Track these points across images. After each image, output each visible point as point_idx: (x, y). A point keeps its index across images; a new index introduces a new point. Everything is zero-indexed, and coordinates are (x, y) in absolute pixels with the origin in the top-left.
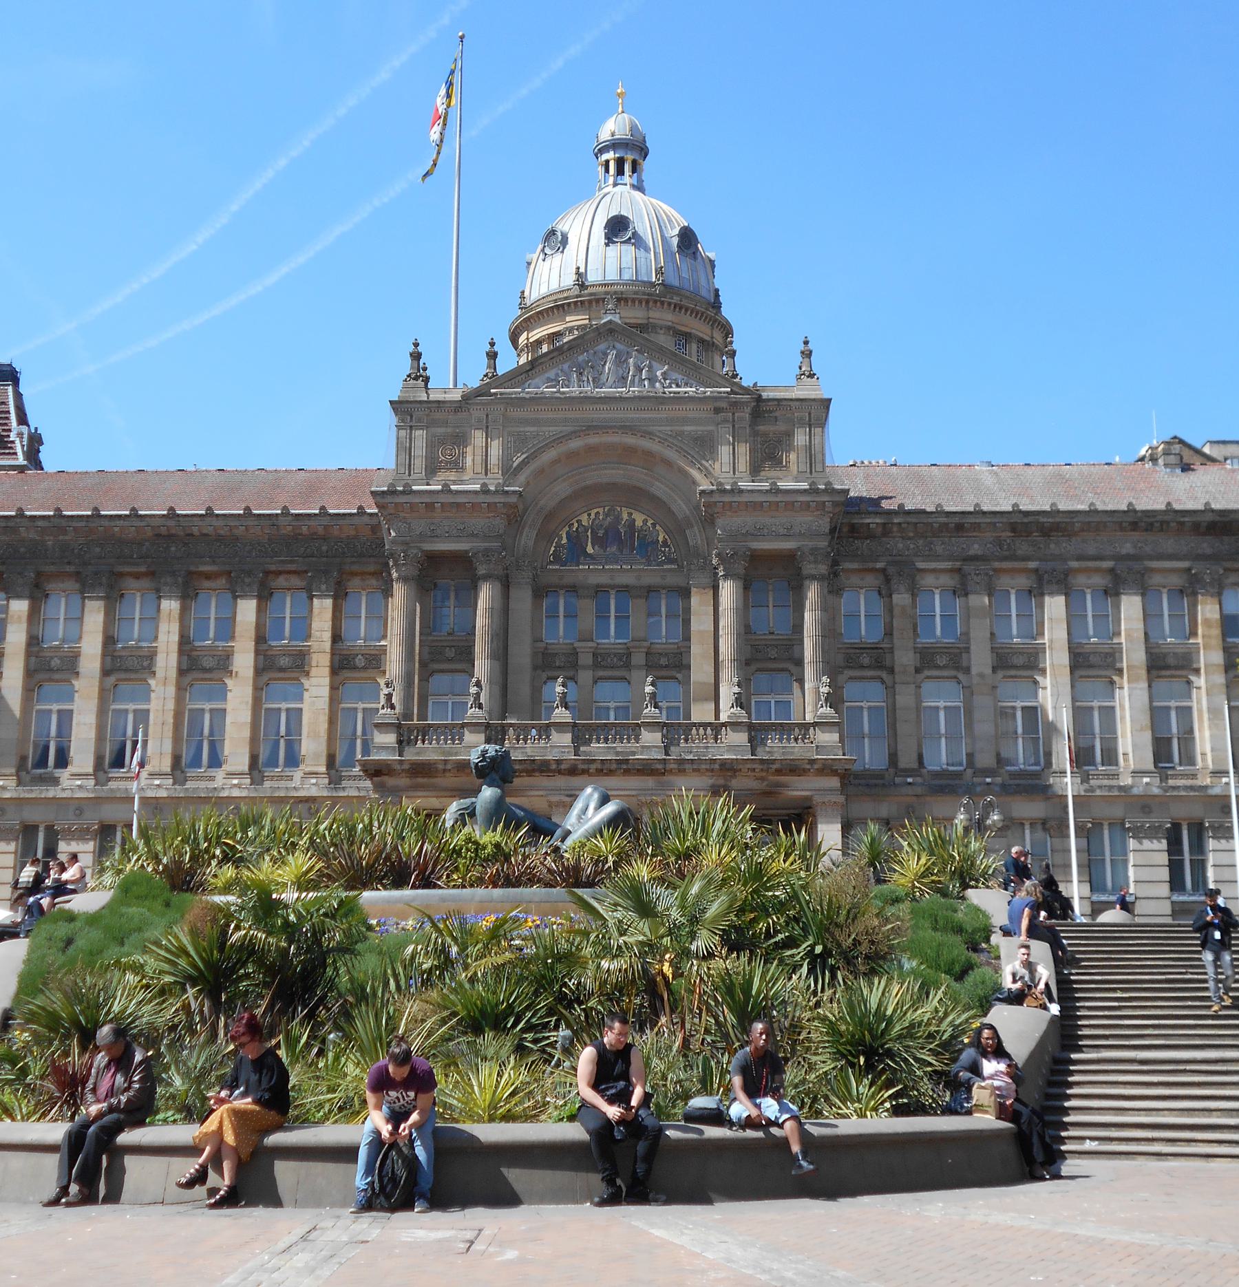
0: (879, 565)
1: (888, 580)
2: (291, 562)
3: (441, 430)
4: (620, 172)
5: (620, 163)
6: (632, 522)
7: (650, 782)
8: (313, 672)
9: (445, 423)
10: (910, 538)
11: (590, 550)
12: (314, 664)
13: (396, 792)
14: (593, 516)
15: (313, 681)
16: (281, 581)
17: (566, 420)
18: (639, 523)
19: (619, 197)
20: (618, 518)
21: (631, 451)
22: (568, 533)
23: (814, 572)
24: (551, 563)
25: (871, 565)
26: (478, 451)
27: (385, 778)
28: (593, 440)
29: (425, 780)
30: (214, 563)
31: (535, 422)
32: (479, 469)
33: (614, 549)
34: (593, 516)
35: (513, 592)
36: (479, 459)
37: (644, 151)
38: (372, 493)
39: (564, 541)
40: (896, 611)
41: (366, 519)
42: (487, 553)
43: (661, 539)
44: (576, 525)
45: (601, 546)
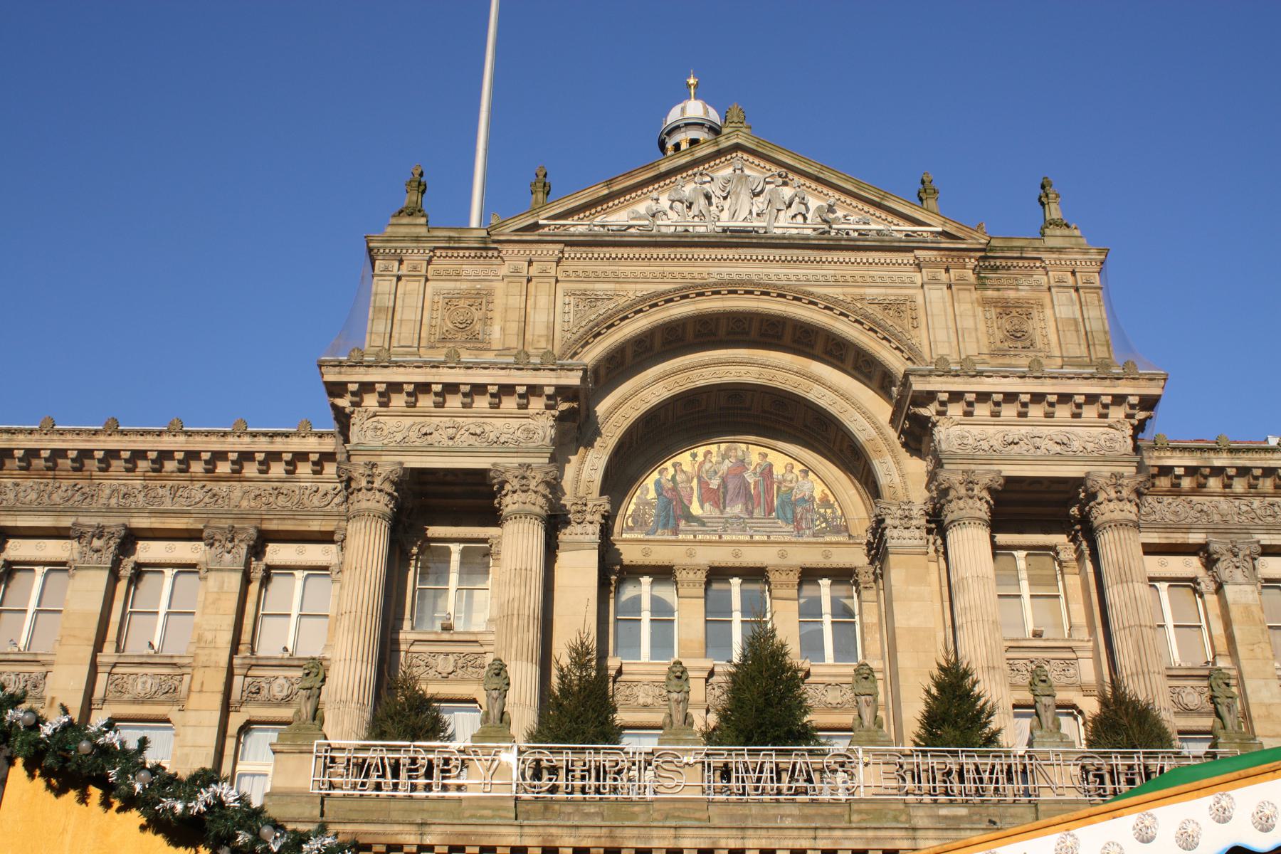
0: (1196, 538)
1: (1210, 562)
6: (767, 471)
8: (194, 700)
9: (457, 276)
10: (1237, 497)
11: (695, 509)
12: (196, 687)
14: (700, 458)
15: (191, 717)
18: (778, 471)
20: (742, 464)
22: (658, 484)
23: (1117, 515)
24: (631, 529)
25: (1178, 538)
26: (515, 315)
31: (616, 278)
32: (513, 342)
33: (736, 509)
34: (700, 458)
35: (564, 559)
36: (513, 327)
38: (326, 383)
39: (652, 494)
40: (1235, 613)
43: (817, 495)
44: (671, 471)
45: (716, 504)
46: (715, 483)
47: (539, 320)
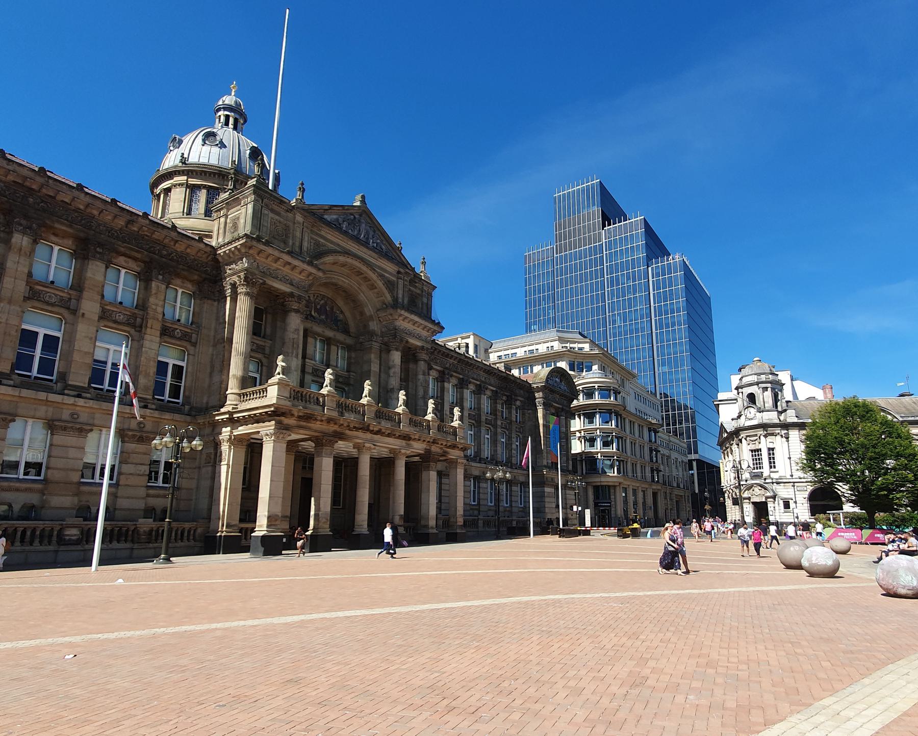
2: (137, 251)
3: (277, 217)
4: (227, 124)
5: (227, 117)
7: (404, 443)
13: (287, 428)
16: (121, 260)
17: (339, 245)
19: (227, 134)
21: (359, 273)
27: (283, 418)
28: (349, 260)
29: (304, 424)
30: (71, 226)
36: (297, 244)
37: (245, 121)
41: (202, 246)
42: (300, 297)
46: (318, 307)
47: (305, 244)
